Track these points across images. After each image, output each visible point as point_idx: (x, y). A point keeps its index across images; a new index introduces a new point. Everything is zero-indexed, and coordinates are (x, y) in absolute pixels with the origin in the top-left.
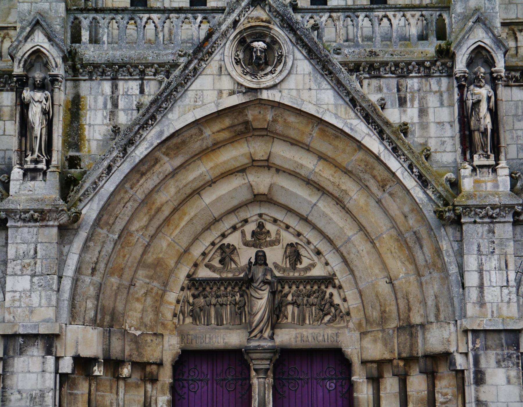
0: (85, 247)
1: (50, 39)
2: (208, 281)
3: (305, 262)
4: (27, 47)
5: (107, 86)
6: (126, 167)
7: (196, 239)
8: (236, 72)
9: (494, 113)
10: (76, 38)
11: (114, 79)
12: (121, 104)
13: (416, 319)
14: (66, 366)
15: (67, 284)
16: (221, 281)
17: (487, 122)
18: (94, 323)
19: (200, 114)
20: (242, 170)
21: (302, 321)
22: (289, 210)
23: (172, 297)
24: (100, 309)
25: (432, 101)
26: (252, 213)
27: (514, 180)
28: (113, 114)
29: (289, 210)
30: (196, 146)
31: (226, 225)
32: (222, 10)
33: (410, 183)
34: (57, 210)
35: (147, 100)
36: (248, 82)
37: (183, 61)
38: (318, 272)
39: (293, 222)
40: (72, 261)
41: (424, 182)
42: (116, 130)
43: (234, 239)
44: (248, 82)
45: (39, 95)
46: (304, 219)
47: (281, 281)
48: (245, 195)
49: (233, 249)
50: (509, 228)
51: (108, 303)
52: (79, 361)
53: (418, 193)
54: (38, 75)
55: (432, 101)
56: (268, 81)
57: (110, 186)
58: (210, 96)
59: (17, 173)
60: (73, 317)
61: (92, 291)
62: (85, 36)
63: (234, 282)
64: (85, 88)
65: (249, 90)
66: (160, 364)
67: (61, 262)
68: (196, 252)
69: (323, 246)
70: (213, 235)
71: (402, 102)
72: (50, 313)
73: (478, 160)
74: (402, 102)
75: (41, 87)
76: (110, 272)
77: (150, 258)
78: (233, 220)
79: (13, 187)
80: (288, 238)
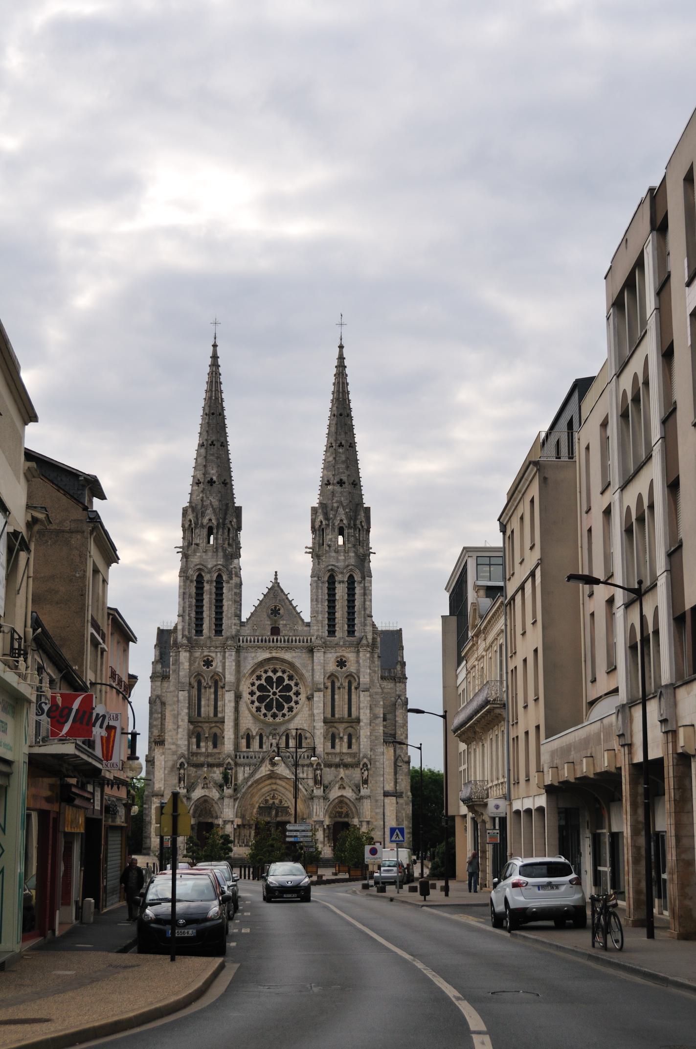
0: (239, 803)
1: (232, 759)
2: (263, 807)
3: (283, 803)
4: (227, 761)
5: (243, 768)
6: (245, 788)
7: (260, 798)
8: (269, 767)
9: (321, 776)
10: (236, 757)
11: (244, 767)
12: (246, 772)
13: (305, 817)
14: (235, 827)
15: (235, 810)
16: (265, 807)
17: (319, 778)
18: (240, 818)
19: (262, 775)
20: (270, 784)
21: (282, 816)
22: (280, 792)
23: (255, 810)
24: (241, 815)
25: (310, 772)
26: (272, 793)
27: (324, 790)
28: (244, 775)
29: (280, 792)
30: (261, 781)
31: (266, 795)
32: (266, 752)
33: (304, 790)
34: (233, 796)
35: (251, 772)
36: (271, 768)
37: (258, 763)
38: (285, 805)
39: (281, 795)
40: (236, 805)
41: (306, 791)
42: (244, 779)
43: (268, 798)
44: (271, 768)
45: (229, 771)
46: (283, 794)
47: (278, 807)
48: (270, 789)
49: (268, 800)
50: (322, 801)
51: (243, 812)
52: (238, 825)
53: (305, 793)
54: (229, 767)
55: (310, 772)
56: (275, 768)
57: (243, 790)
58: (264, 771)
59: (225, 788)
60: (237, 817)
61: (240, 811)
62: (238, 757)
63: (269, 807)
64: (238, 769)
65: (272, 770)
66: (252, 825)
67: (234, 805)
68: (260, 801)
69: (287, 800)
70: (264, 797)
71: (303, 772)
72: (232, 816)
73: (317, 786)
74: (303, 772)
75: (229, 770)
76: (243, 807)
77: (251, 803)
78: (268, 794)
79: (225, 791)
80: (279, 798)
